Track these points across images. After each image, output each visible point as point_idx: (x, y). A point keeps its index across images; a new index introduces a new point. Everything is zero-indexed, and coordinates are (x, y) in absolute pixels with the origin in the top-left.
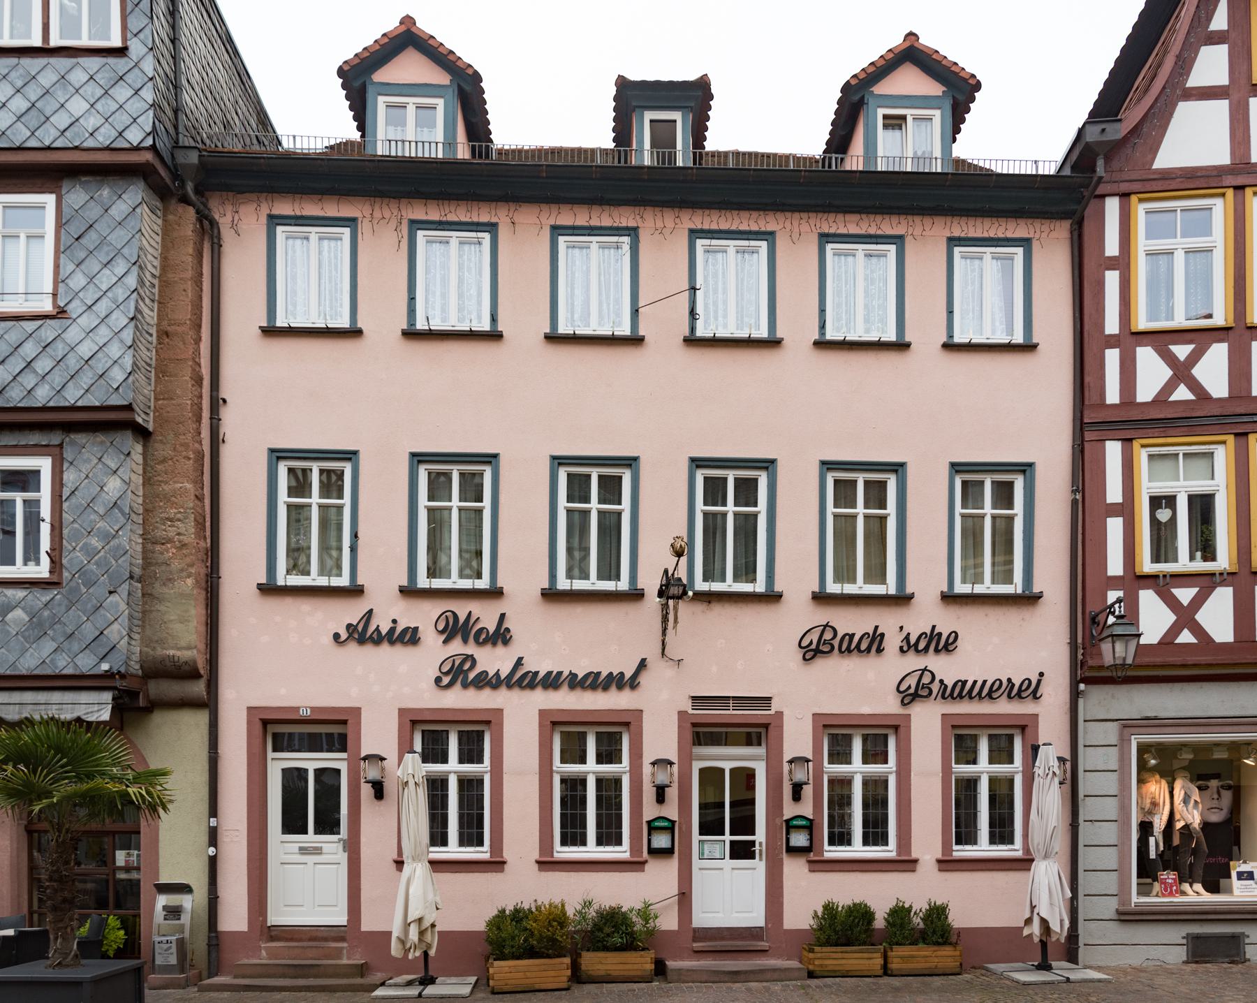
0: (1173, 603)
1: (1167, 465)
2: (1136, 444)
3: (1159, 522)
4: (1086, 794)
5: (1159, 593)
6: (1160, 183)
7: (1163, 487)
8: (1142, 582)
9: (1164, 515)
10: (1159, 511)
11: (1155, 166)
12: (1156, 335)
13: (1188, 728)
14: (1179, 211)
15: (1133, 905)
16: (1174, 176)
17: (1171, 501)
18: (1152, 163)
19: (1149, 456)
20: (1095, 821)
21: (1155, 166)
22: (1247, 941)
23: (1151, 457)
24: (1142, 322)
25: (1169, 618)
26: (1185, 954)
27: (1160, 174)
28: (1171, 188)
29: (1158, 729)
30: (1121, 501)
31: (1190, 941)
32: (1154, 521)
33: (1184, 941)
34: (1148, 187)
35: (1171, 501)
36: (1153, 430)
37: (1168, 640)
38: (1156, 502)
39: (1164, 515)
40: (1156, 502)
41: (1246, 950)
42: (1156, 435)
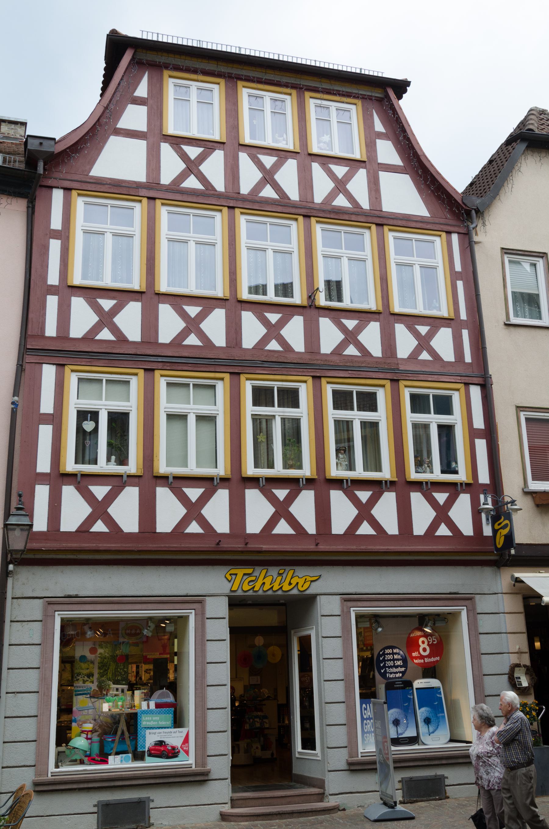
0: (89, 498)
1: (94, 387)
2: (67, 369)
3: (84, 431)
4: (10, 667)
5: (78, 489)
6: (93, 186)
7: (88, 404)
8: (66, 479)
9: (89, 426)
10: (85, 422)
11: (91, 174)
12: (87, 290)
13: (112, 605)
14: (109, 206)
15: (50, 775)
16: (105, 182)
17: (94, 415)
18: (89, 172)
19: (79, 379)
20: (18, 693)
21: (91, 174)
22: (152, 805)
23: (80, 380)
24: (77, 279)
25: (86, 510)
26: (96, 822)
27: (95, 179)
28: (102, 190)
29: (79, 606)
30: (52, 412)
31: (100, 808)
32: (80, 430)
33: (95, 809)
34: (85, 186)
35: (94, 415)
36: (81, 360)
37: (84, 529)
38: (82, 415)
39: (89, 426)
40: (82, 415)
41: (151, 815)
42: (83, 364)
